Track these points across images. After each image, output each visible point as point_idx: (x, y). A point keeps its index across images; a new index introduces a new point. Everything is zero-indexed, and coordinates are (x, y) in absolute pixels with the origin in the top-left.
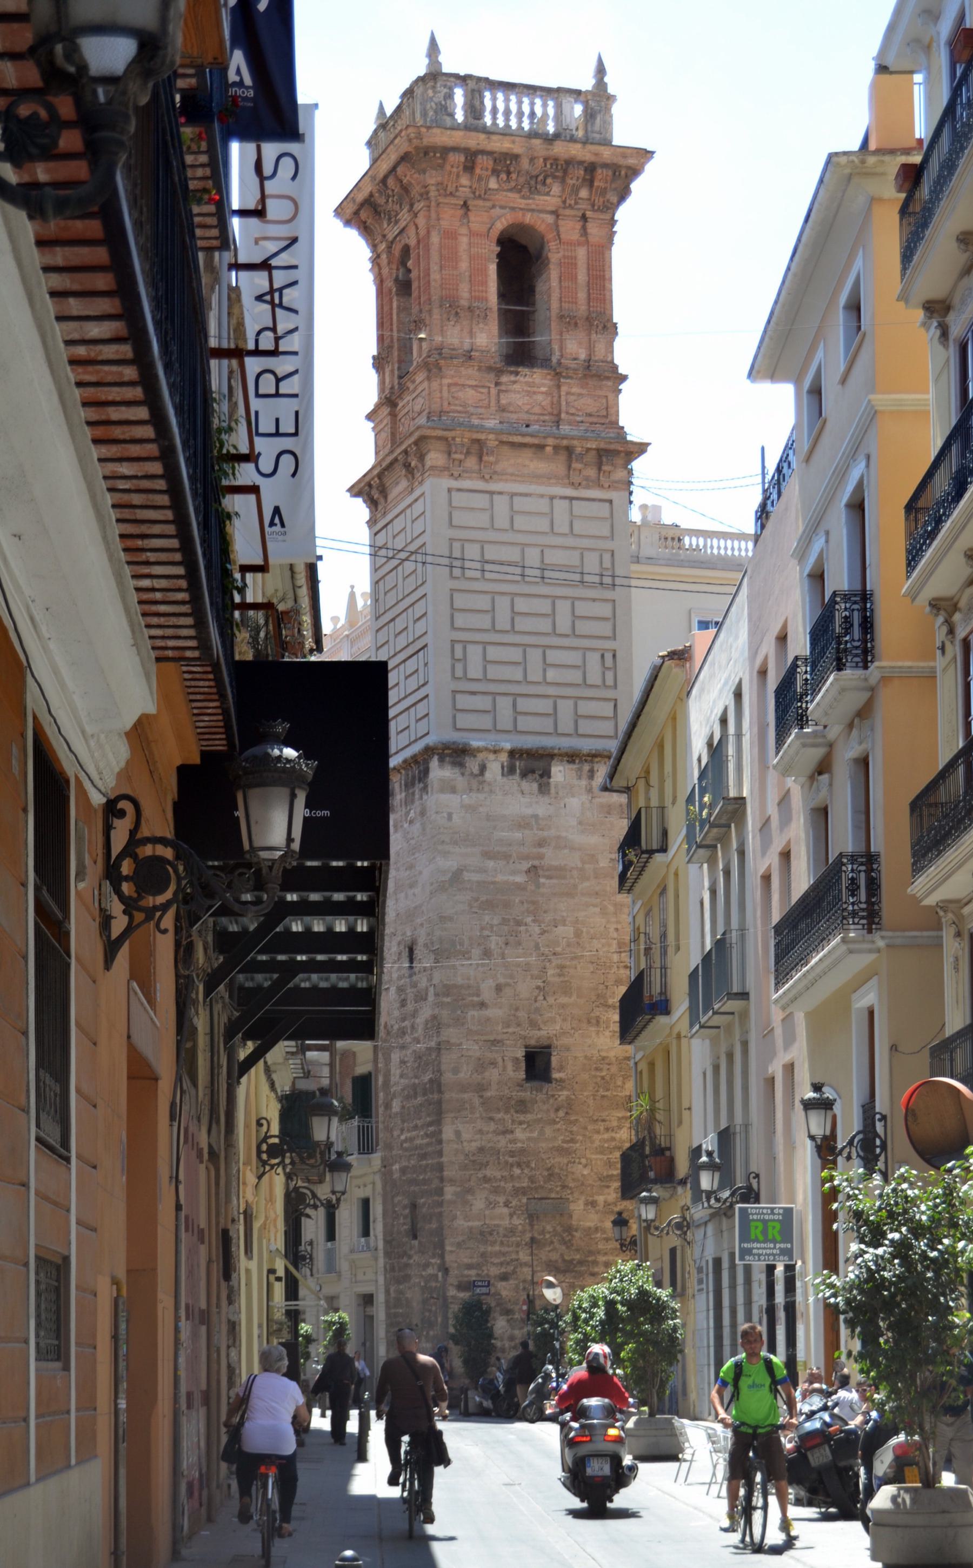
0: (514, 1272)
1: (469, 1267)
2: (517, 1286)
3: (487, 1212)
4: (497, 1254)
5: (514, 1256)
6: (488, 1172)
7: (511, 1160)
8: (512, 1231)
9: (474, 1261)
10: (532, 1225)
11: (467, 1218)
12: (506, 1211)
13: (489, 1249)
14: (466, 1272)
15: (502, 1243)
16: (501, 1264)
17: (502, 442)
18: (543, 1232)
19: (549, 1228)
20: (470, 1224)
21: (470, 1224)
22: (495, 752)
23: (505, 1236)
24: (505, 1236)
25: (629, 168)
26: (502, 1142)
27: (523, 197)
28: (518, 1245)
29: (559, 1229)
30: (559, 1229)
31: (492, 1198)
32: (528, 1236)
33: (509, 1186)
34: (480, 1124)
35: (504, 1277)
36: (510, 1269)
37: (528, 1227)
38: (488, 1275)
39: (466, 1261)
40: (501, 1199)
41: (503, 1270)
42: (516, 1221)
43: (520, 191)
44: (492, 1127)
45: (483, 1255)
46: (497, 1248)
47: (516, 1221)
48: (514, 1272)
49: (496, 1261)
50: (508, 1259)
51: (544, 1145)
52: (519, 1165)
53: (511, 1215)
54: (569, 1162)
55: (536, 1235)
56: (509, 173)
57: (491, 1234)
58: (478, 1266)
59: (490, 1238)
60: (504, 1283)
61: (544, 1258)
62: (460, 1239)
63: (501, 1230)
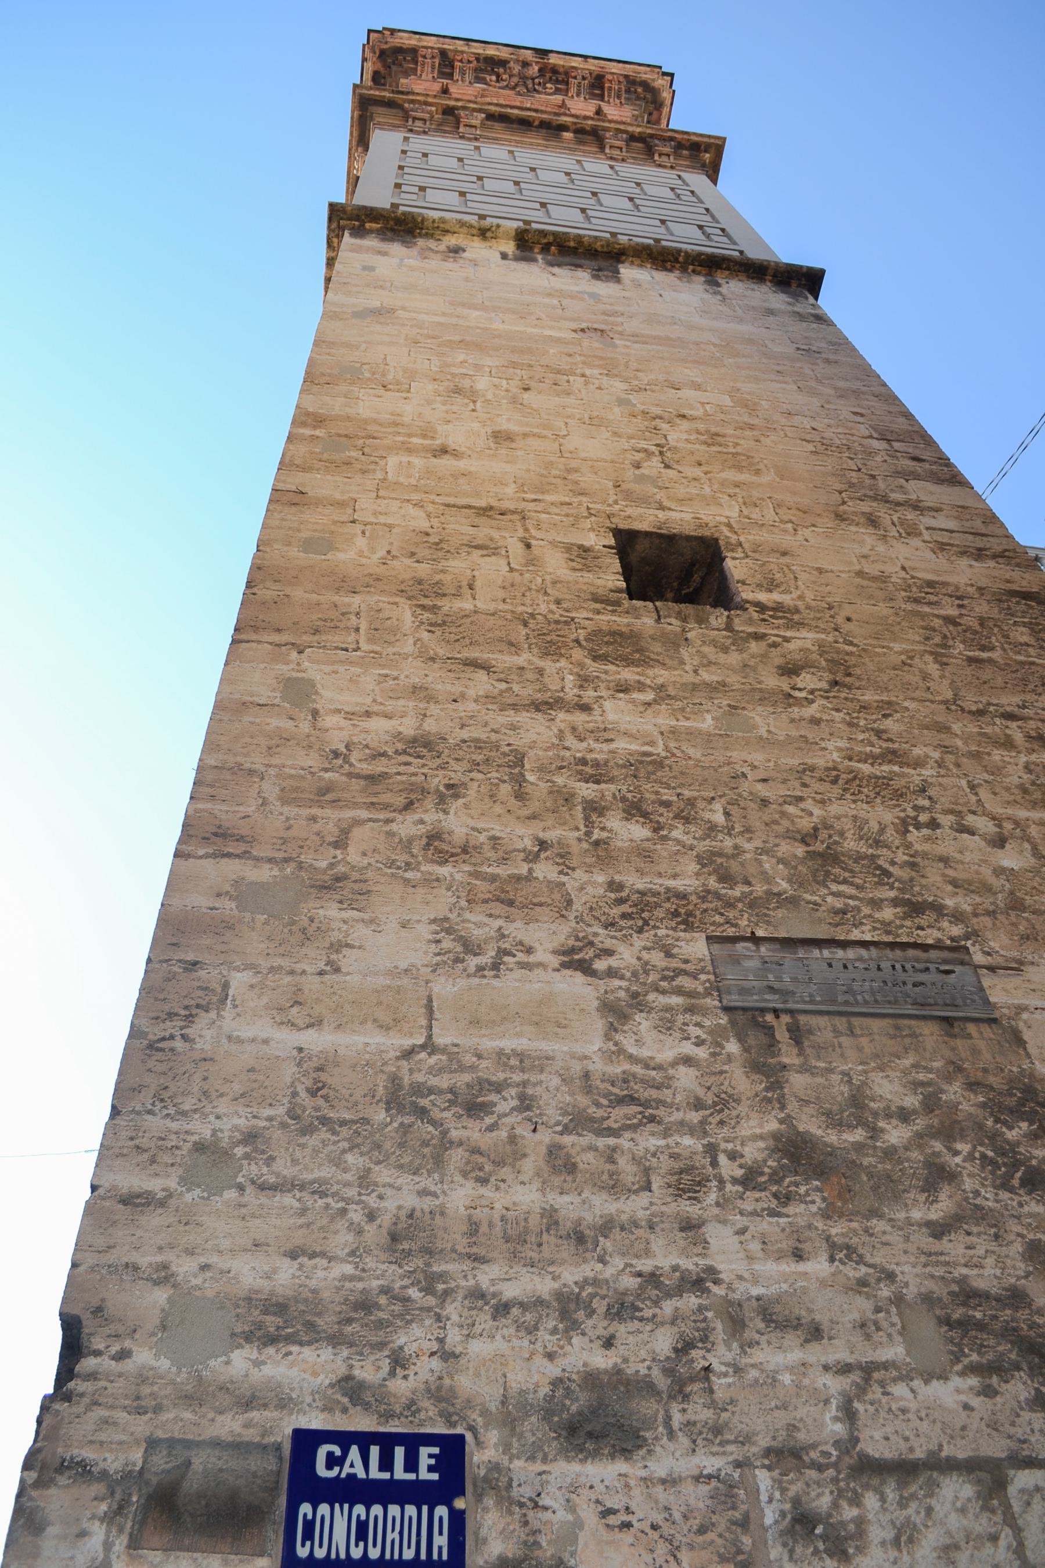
0: (683, 1378)
1: (277, 1322)
2: (726, 1491)
3: (444, 988)
4: (519, 1240)
5: (666, 1256)
6: (457, 823)
7: (586, 790)
8: (635, 1099)
9: (327, 1277)
10: (767, 1070)
11: (294, 1008)
12: (575, 986)
13: (460, 1196)
14: (240, 1363)
15: (561, 1165)
16: (569, 1308)
17: (491, 117)
18: (857, 1108)
19: (888, 1088)
20: (315, 1040)
21: (311, 1039)
22: (484, 233)
23: (578, 1122)
24: (578, 1122)
25: (645, 85)
26: (535, 732)
27: (519, 94)
28: (688, 1182)
29: (964, 1102)
30: (964, 1102)
31: (480, 925)
32: (753, 1132)
33: (588, 885)
34: (413, 672)
35: (597, 1422)
36: (646, 1347)
37: (742, 1082)
38: (440, 1394)
39: (249, 1273)
40: (545, 936)
41: (583, 1355)
42: (649, 1042)
43: (514, 88)
44: (481, 683)
45: (405, 1237)
46: (524, 1195)
47: (649, 1042)
48: (683, 1378)
49: (524, 1284)
50: (617, 1271)
51: (757, 757)
52: (635, 810)
53: (616, 1014)
54: (904, 826)
55: (810, 1124)
56: (498, 76)
57: (475, 1109)
58: (363, 1317)
59: (472, 1131)
60: (603, 1472)
61: (913, 1278)
62: (229, 1120)
63: (554, 1097)
